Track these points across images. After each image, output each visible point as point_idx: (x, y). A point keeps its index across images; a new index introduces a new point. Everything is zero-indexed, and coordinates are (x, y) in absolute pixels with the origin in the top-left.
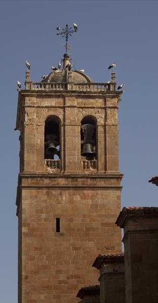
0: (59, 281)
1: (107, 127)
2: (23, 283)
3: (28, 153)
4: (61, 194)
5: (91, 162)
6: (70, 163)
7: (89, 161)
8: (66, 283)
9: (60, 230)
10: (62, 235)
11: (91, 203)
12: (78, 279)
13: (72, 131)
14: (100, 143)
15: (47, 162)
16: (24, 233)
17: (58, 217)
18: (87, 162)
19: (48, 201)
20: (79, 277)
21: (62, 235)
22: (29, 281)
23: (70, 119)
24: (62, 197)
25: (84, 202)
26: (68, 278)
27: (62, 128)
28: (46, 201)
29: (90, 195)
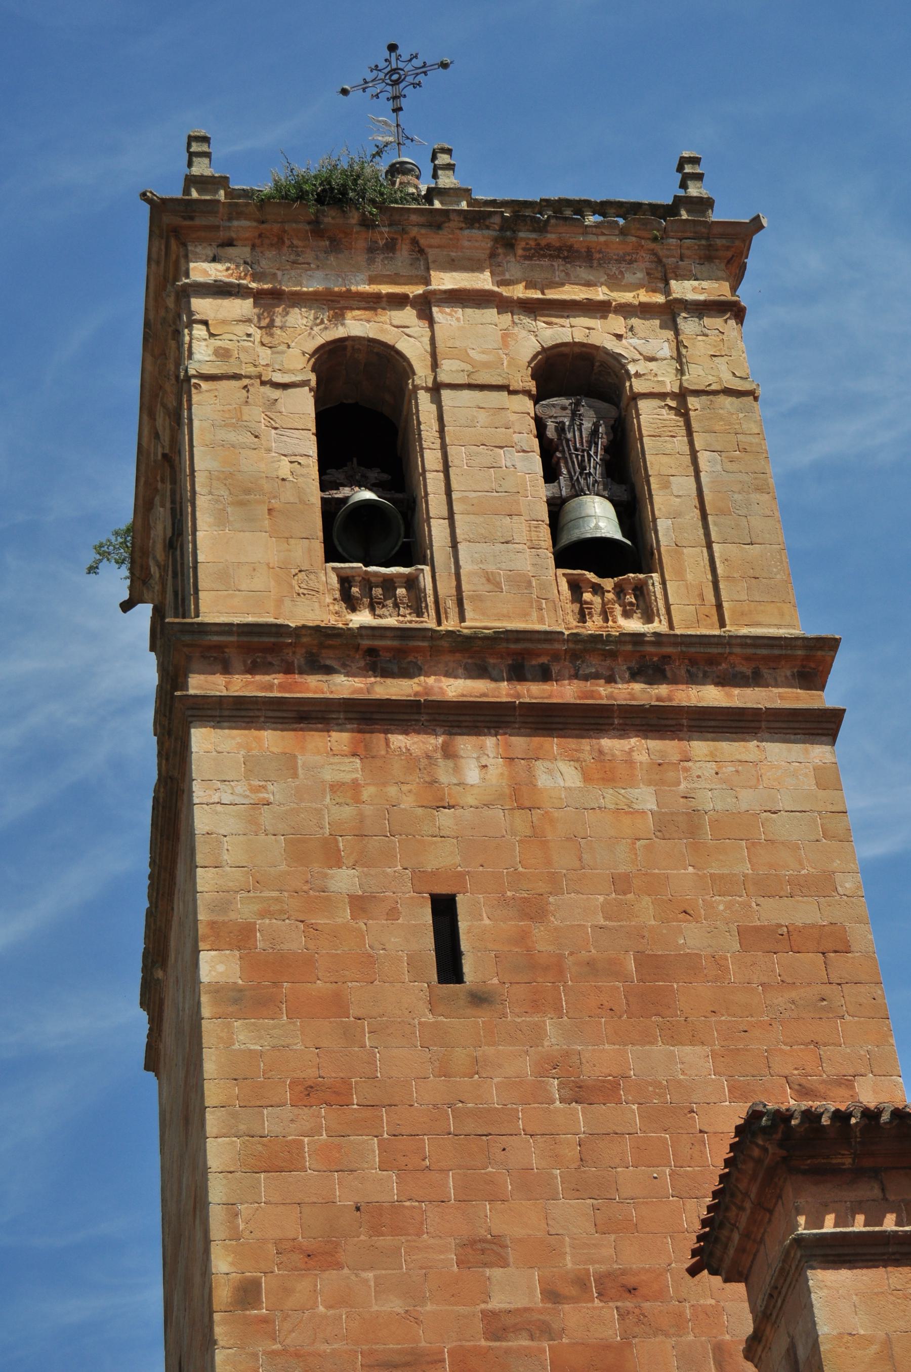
0: (490, 1317)
1: (692, 402)
2: (219, 1331)
3: (221, 520)
4: (448, 753)
5: (620, 591)
6: (490, 578)
7: (608, 583)
8: (545, 1330)
9: (466, 969)
10: (479, 999)
11: (651, 804)
12: (628, 1304)
13: (482, 417)
14: (666, 485)
15: (345, 582)
16: (217, 989)
17: (442, 889)
18: (597, 589)
19: (367, 793)
20: (631, 1290)
21: (479, 999)
22: (264, 1320)
23: (464, 356)
24: (457, 770)
25: (609, 797)
26: (552, 1295)
27: (425, 405)
28: (355, 786)
29: (641, 757)
